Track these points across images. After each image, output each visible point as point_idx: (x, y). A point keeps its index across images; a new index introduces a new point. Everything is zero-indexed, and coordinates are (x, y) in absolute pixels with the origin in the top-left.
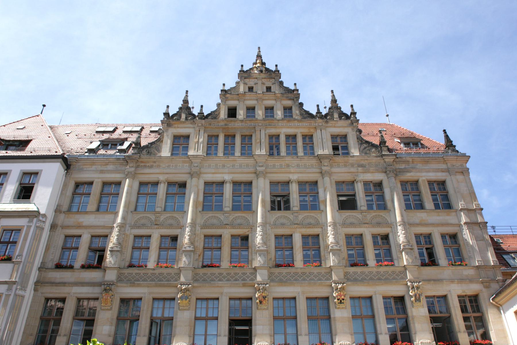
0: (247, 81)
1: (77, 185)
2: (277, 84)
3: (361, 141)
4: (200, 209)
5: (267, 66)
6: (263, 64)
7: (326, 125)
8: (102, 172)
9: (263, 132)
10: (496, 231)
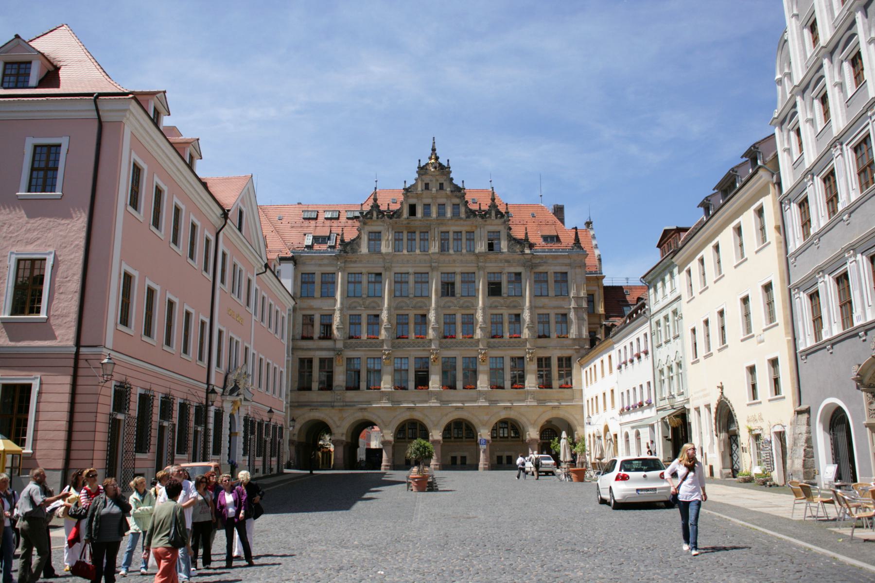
3: (511, 239)
5: (440, 160)
6: (437, 158)
8: (320, 265)
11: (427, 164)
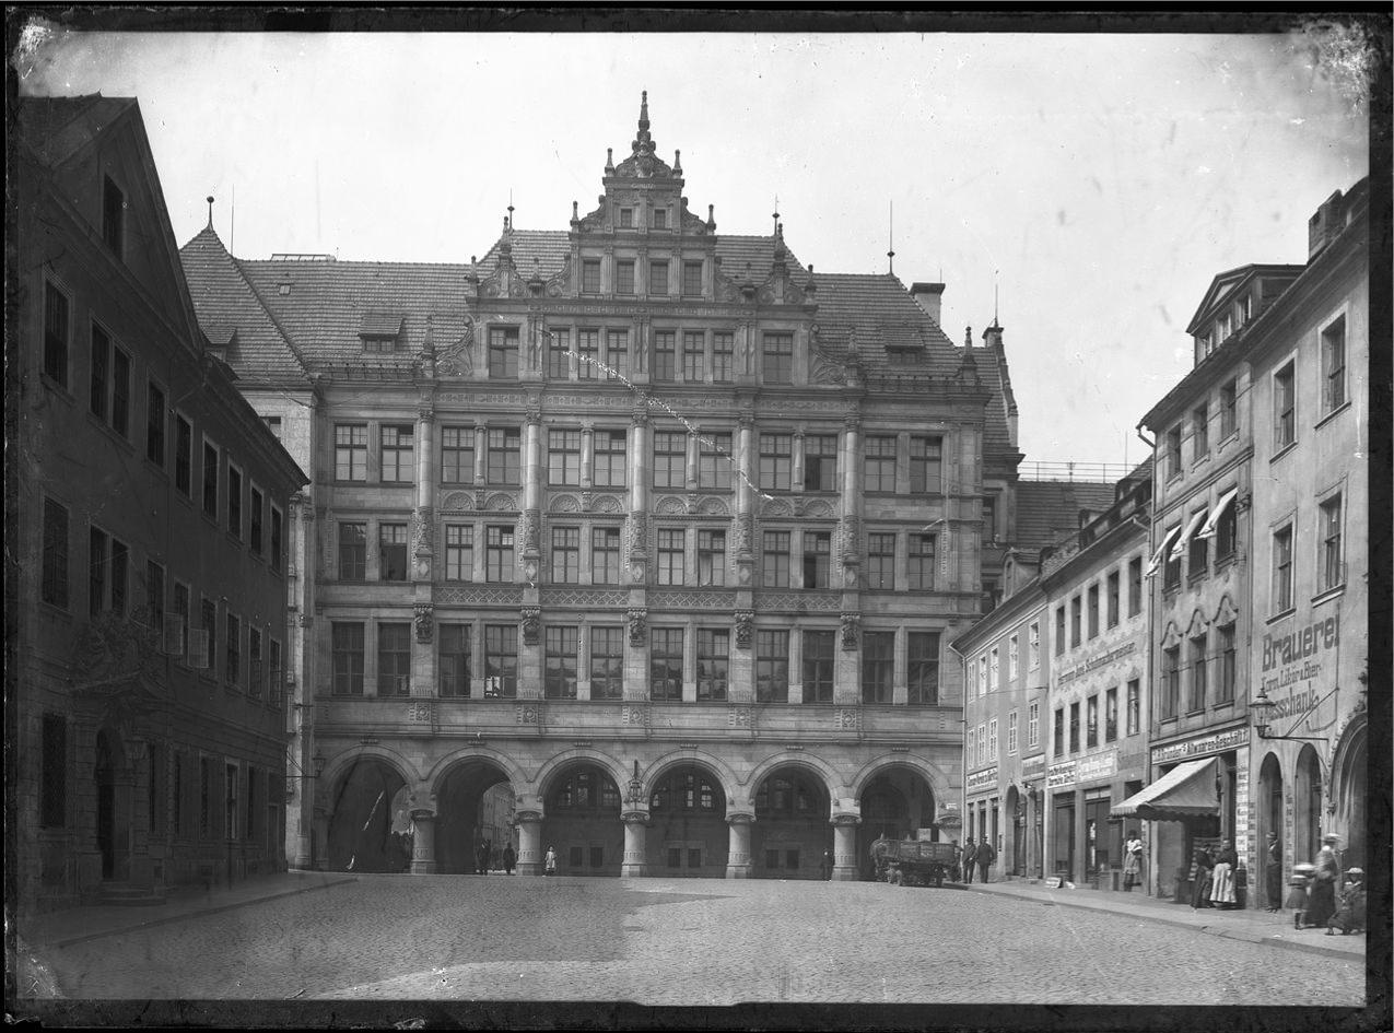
6: (652, 146)
7: (761, 314)
8: (376, 407)
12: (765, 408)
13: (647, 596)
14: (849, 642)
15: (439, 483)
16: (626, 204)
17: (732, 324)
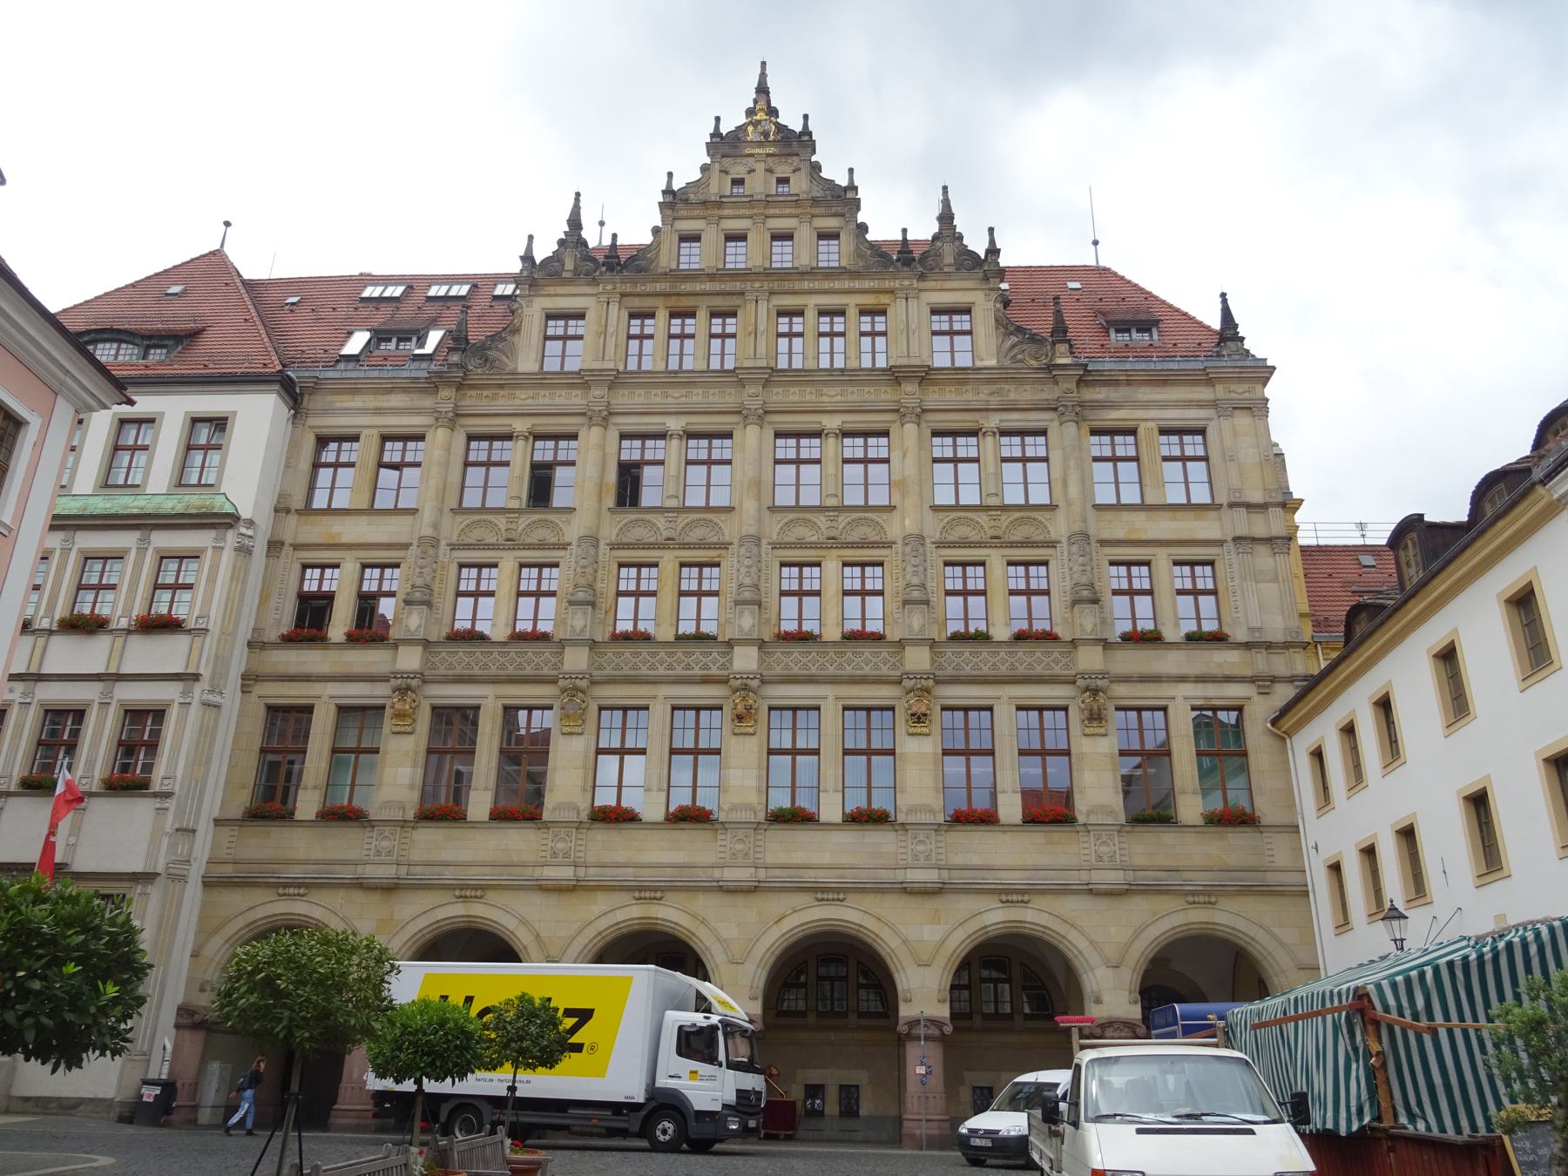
0: (726, 161)
1: (322, 441)
2: (803, 172)
4: (610, 501)
6: (773, 112)
7: (922, 285)
8: (379, 411)
9: (763, 306)
10: (1368, 534)
11: (741, 129)
12: (936, 396)
13: (760, 658)
14: (1095, 717)
15: (455, 505)
16: (738, 171)
17: (884, 299)
